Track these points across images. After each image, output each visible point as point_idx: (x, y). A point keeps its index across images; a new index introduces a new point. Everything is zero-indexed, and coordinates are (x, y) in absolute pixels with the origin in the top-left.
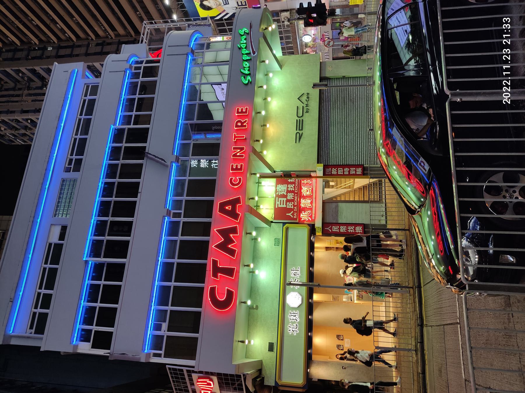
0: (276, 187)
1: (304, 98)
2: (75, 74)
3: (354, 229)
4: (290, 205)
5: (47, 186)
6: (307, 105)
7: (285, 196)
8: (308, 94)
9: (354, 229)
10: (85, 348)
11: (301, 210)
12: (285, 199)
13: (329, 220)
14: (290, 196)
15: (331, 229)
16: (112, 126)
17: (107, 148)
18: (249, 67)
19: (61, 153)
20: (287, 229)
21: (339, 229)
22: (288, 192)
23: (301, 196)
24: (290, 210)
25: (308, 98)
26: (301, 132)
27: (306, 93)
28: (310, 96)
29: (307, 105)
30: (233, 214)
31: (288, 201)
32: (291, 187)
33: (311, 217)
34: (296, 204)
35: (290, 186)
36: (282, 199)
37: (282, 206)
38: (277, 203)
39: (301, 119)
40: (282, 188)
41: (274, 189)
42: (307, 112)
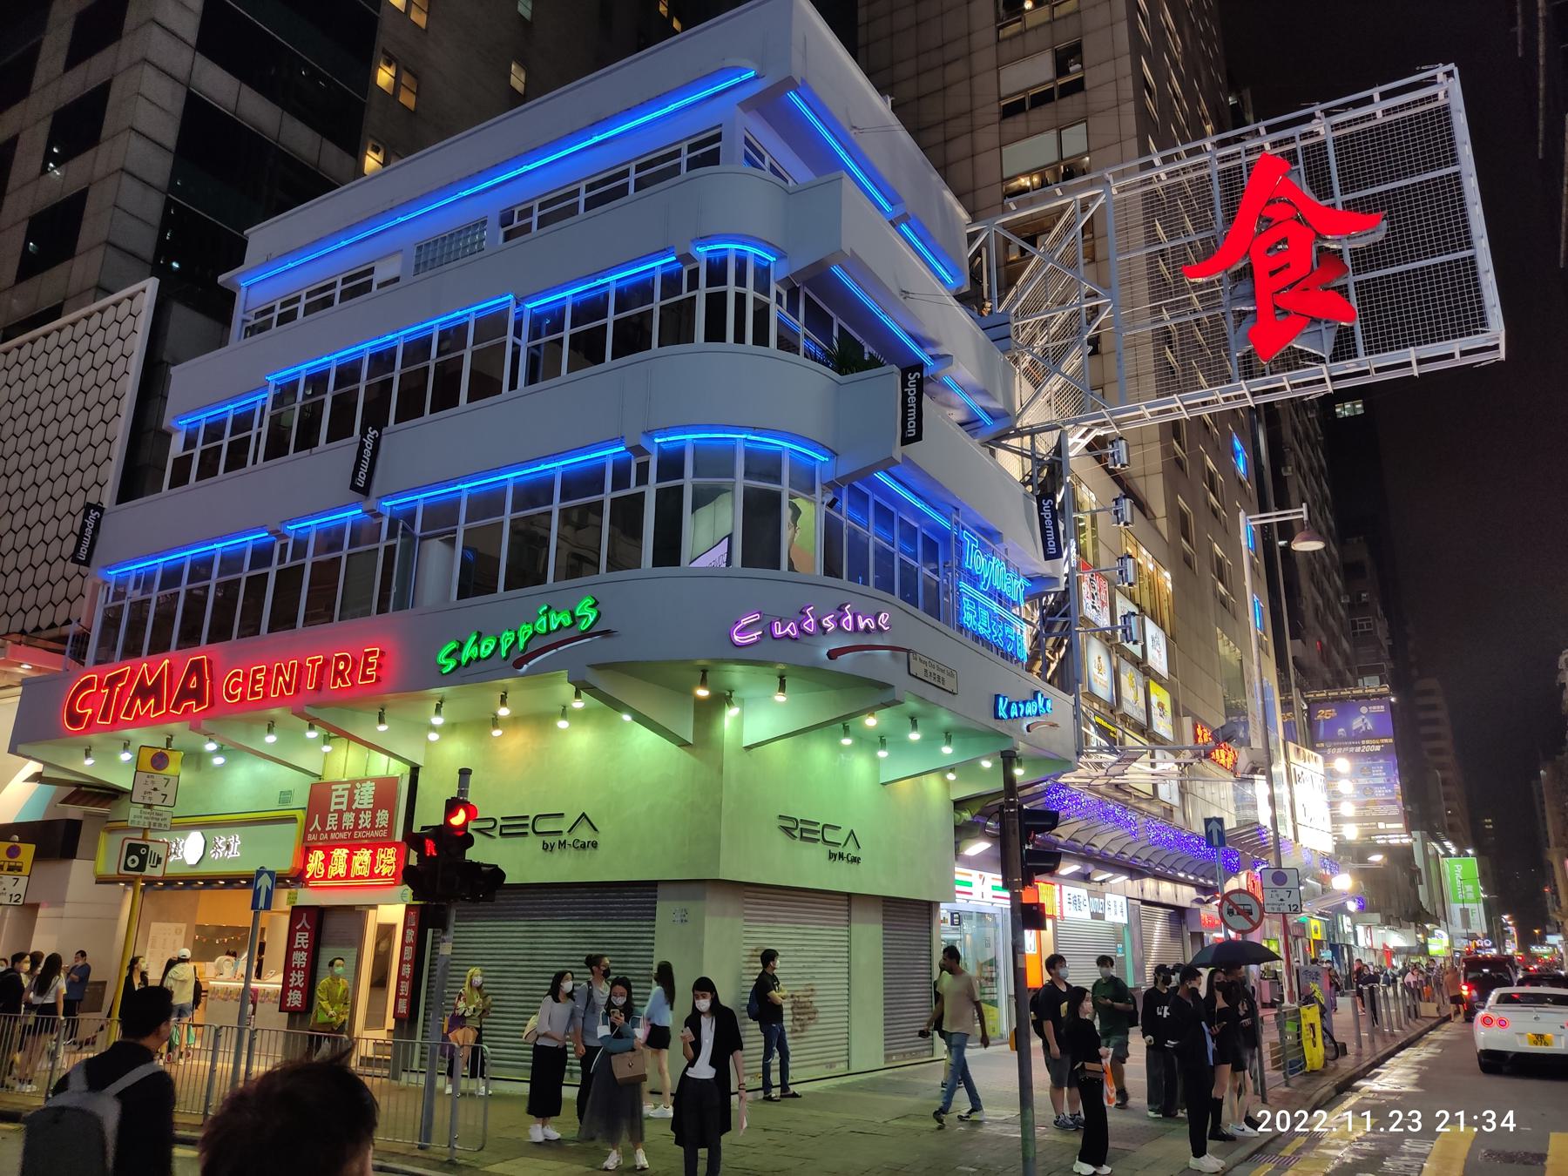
0: (372, 780)
1: (584, 834)
2: (737, 80)
3: (297, 988)
4: (332, 821)
5: (465, 194)
6: (562, 844)
7: (349, 809)
8: (595, 845)
9: (297, 988)
10: (176, 448)
11: (328, 850)
12: (344, 807)
13: (332, 924)
14: (348, 819)
15: (303, 929)
16: (510, 297)
17: (458, 314)
18: (479, 658)
19: (539, 173)
20: (293, 820)
21: (301, 949)
22: (358, 811)
23: (353, 848)
24: (323, 823)
25: (584, 846)
26: (496, 833)
27: (600, 839)
28: (588, 852)
29: (562, 844)
30: (186, 694)
31: (340, 813)
32: (365, 818)
33: (312, 878)
34: (333, 836)
35: (368, 816)
36: (345, 800)
37: (334, 800)
38: (340, 787)
39: (529, 830)
40: (365, 797)
41: (340, 777)
42: (546, 847)
